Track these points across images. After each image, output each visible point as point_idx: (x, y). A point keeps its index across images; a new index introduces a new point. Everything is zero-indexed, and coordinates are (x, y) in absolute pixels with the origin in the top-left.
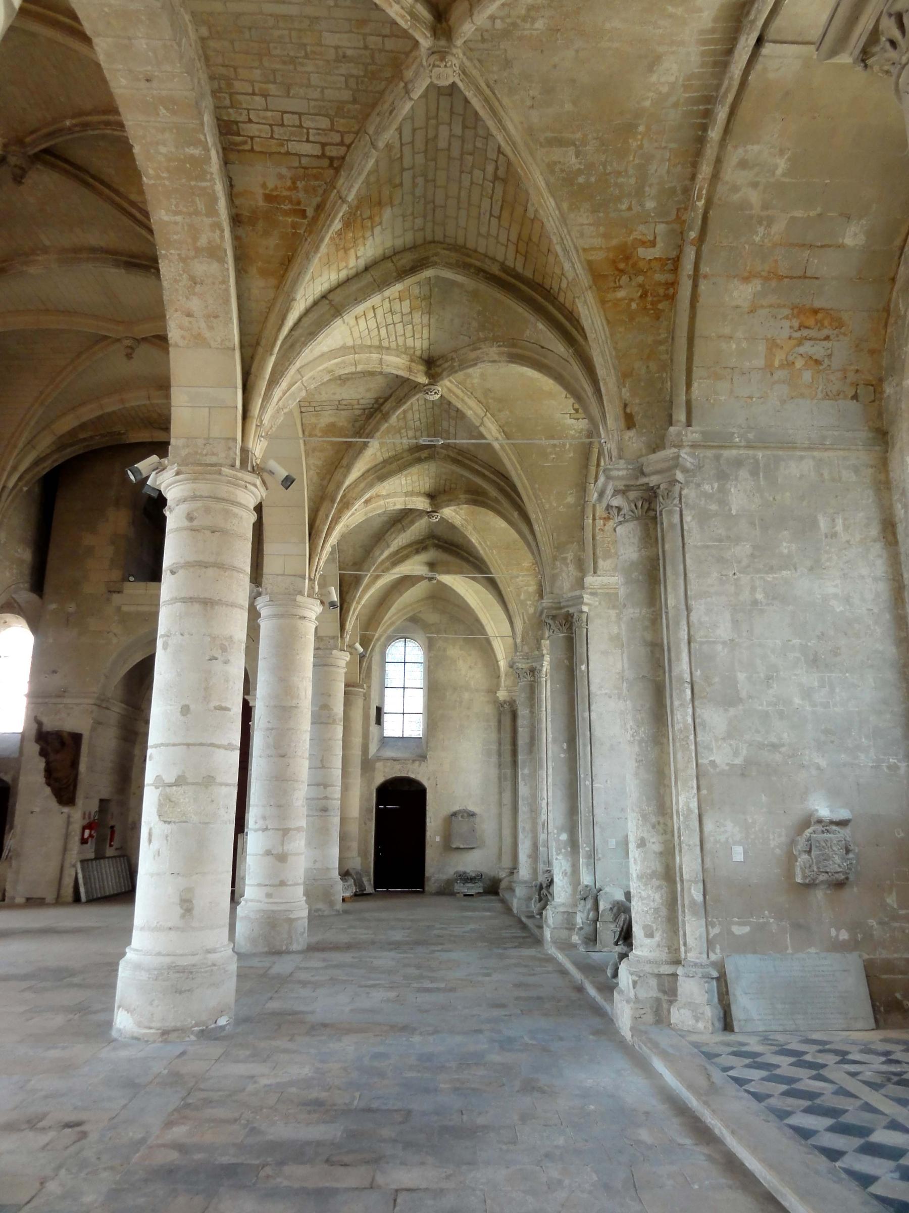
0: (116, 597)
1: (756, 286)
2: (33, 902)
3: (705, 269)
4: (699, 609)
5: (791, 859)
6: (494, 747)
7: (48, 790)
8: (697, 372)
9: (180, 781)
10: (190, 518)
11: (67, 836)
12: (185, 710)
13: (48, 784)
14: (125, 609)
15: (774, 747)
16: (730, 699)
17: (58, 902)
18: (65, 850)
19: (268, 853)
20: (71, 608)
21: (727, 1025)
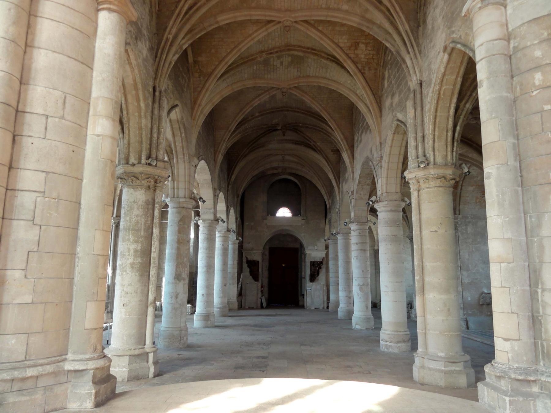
0: (265, 221)
1: (474, 187)
2: (251, 308)
3: (464, 184)
4: (461, 252)
5: (479, 300)
6: (374, 263)
7: (251, 277)
8: (461, 203)
9: (363, 285)
10: (360, 233)
11: (258, 290)
12: (363, 271)
13: (251, 275)
14: (268, 224)
15: (476, 279)
16: (468, 270)
17: (257, 308)
18: (257, 294)
19: (347, 296)
20: (252, 224)
21: (468, 328)
